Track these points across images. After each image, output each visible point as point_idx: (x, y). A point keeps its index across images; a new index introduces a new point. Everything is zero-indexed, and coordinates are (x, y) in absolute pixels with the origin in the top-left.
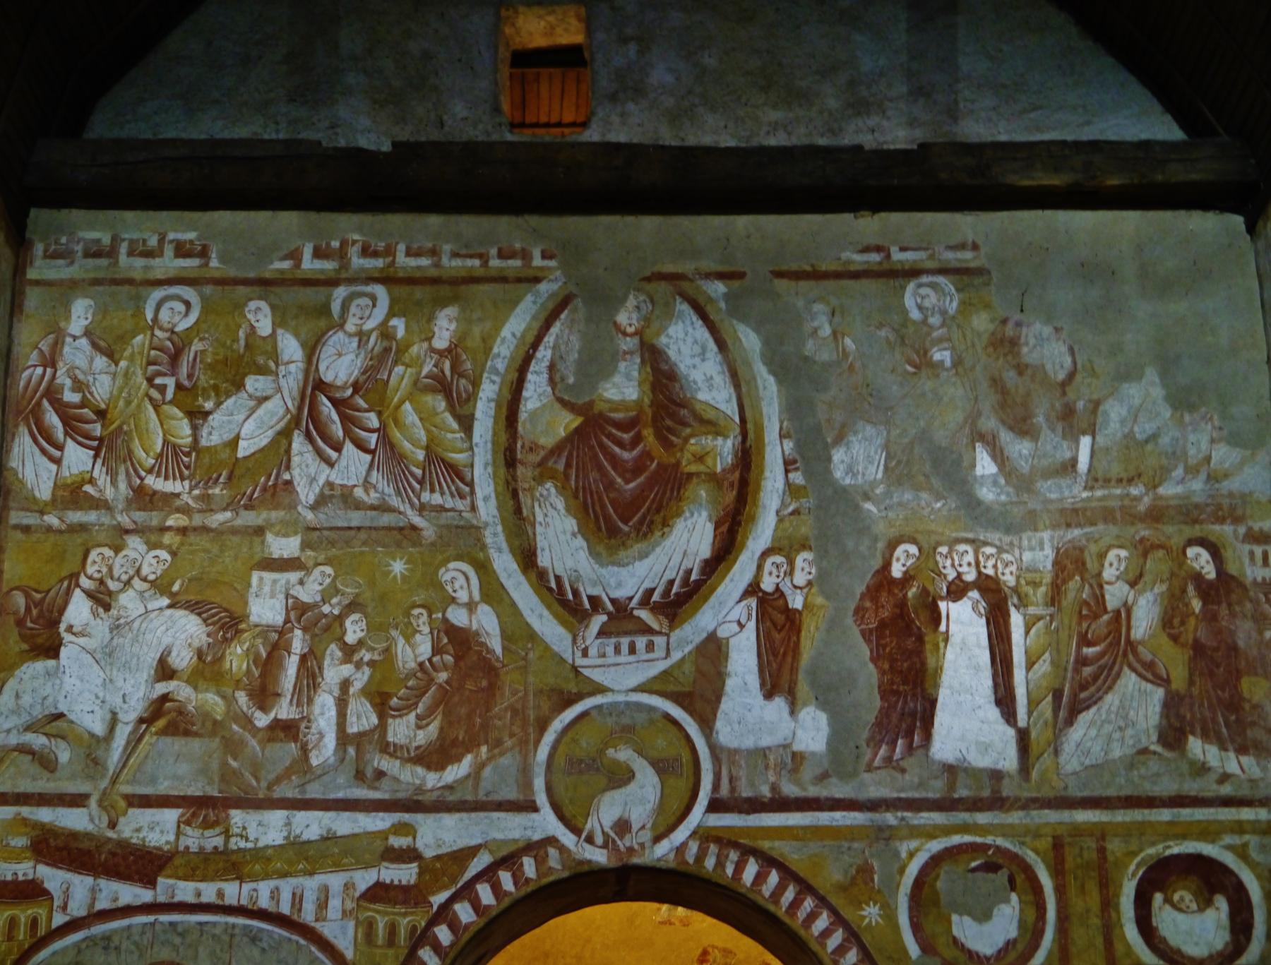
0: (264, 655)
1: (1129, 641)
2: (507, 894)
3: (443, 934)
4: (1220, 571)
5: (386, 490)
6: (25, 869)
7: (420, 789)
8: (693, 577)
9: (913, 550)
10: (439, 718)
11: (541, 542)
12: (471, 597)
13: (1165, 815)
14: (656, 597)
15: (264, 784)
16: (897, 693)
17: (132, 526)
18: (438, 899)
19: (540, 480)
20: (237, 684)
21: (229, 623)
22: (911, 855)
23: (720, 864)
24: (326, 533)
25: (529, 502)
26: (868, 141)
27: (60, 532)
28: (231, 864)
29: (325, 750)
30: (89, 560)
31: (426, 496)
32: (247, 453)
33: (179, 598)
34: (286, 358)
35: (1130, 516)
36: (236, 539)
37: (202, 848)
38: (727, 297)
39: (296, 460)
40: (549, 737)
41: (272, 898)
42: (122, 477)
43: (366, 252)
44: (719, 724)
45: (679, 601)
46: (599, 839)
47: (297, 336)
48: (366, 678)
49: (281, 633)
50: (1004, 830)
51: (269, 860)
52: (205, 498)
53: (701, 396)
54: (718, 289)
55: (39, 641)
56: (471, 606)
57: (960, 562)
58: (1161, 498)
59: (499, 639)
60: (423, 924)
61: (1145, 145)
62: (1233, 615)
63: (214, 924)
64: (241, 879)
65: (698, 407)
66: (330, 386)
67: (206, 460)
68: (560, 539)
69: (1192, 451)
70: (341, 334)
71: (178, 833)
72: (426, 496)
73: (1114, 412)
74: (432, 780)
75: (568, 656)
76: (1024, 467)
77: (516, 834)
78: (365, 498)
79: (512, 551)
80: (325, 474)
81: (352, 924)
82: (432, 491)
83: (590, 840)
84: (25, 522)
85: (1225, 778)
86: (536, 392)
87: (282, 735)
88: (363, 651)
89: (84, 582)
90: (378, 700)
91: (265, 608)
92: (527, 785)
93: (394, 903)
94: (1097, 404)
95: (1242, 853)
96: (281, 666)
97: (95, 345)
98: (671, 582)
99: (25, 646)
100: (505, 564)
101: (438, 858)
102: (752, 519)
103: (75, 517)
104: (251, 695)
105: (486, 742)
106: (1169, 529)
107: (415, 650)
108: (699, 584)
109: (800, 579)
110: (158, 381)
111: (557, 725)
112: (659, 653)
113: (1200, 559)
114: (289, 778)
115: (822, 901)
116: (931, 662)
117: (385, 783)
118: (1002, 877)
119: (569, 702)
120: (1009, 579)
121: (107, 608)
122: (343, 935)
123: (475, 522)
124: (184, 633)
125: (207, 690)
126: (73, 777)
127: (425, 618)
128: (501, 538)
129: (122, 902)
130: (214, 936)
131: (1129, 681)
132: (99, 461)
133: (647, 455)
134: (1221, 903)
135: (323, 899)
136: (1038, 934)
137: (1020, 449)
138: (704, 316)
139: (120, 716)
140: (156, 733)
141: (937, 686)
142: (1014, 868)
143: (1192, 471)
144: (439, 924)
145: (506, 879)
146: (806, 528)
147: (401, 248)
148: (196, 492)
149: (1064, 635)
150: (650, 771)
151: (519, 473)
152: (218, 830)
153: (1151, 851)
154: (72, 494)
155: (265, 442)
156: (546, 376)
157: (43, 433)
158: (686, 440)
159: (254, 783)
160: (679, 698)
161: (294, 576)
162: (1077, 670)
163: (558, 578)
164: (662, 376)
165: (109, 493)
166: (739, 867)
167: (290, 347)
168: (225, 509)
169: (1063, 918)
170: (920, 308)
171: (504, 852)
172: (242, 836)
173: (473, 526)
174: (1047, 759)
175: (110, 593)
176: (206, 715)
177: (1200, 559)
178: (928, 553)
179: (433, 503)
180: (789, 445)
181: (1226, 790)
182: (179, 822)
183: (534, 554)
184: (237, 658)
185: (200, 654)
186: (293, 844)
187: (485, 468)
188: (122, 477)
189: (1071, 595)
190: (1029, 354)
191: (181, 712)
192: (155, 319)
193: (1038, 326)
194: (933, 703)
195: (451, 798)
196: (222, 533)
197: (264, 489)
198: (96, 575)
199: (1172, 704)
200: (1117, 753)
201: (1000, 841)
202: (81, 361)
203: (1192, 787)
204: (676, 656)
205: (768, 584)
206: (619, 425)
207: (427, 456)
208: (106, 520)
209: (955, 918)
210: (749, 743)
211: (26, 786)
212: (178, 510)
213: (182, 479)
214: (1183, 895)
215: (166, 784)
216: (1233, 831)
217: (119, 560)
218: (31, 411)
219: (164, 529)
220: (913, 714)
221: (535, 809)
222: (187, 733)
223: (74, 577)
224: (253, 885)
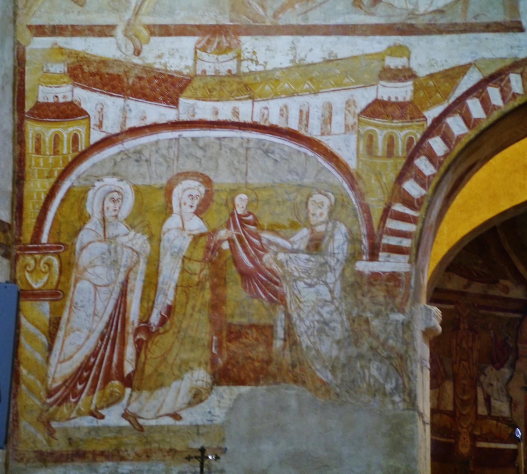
2: (495, 108)
3: (437, 145)
6: (65, 92)
15: (270, 13)
28: (244, 86)
37: (216, 71)
41: (282, 115)
51: (277, 81)
60: (419, 136)
63: (231, 139)
71: (196, 59)
77: (503, 53)
81: (354, 137)
101: (431, 76)
114: (293, 6)
129: (149, 121)
130: (231, 149)
135: (327, 115)
144: (433, 136)
145: (494, 94)
152: (231, 55)
159: (261, 11)
171: (492, 70)
172: (252, 60)
182: (196, 48)
186: (298, 66)
195: (442, 21)
215: (182, 14)
224: (264, 104)
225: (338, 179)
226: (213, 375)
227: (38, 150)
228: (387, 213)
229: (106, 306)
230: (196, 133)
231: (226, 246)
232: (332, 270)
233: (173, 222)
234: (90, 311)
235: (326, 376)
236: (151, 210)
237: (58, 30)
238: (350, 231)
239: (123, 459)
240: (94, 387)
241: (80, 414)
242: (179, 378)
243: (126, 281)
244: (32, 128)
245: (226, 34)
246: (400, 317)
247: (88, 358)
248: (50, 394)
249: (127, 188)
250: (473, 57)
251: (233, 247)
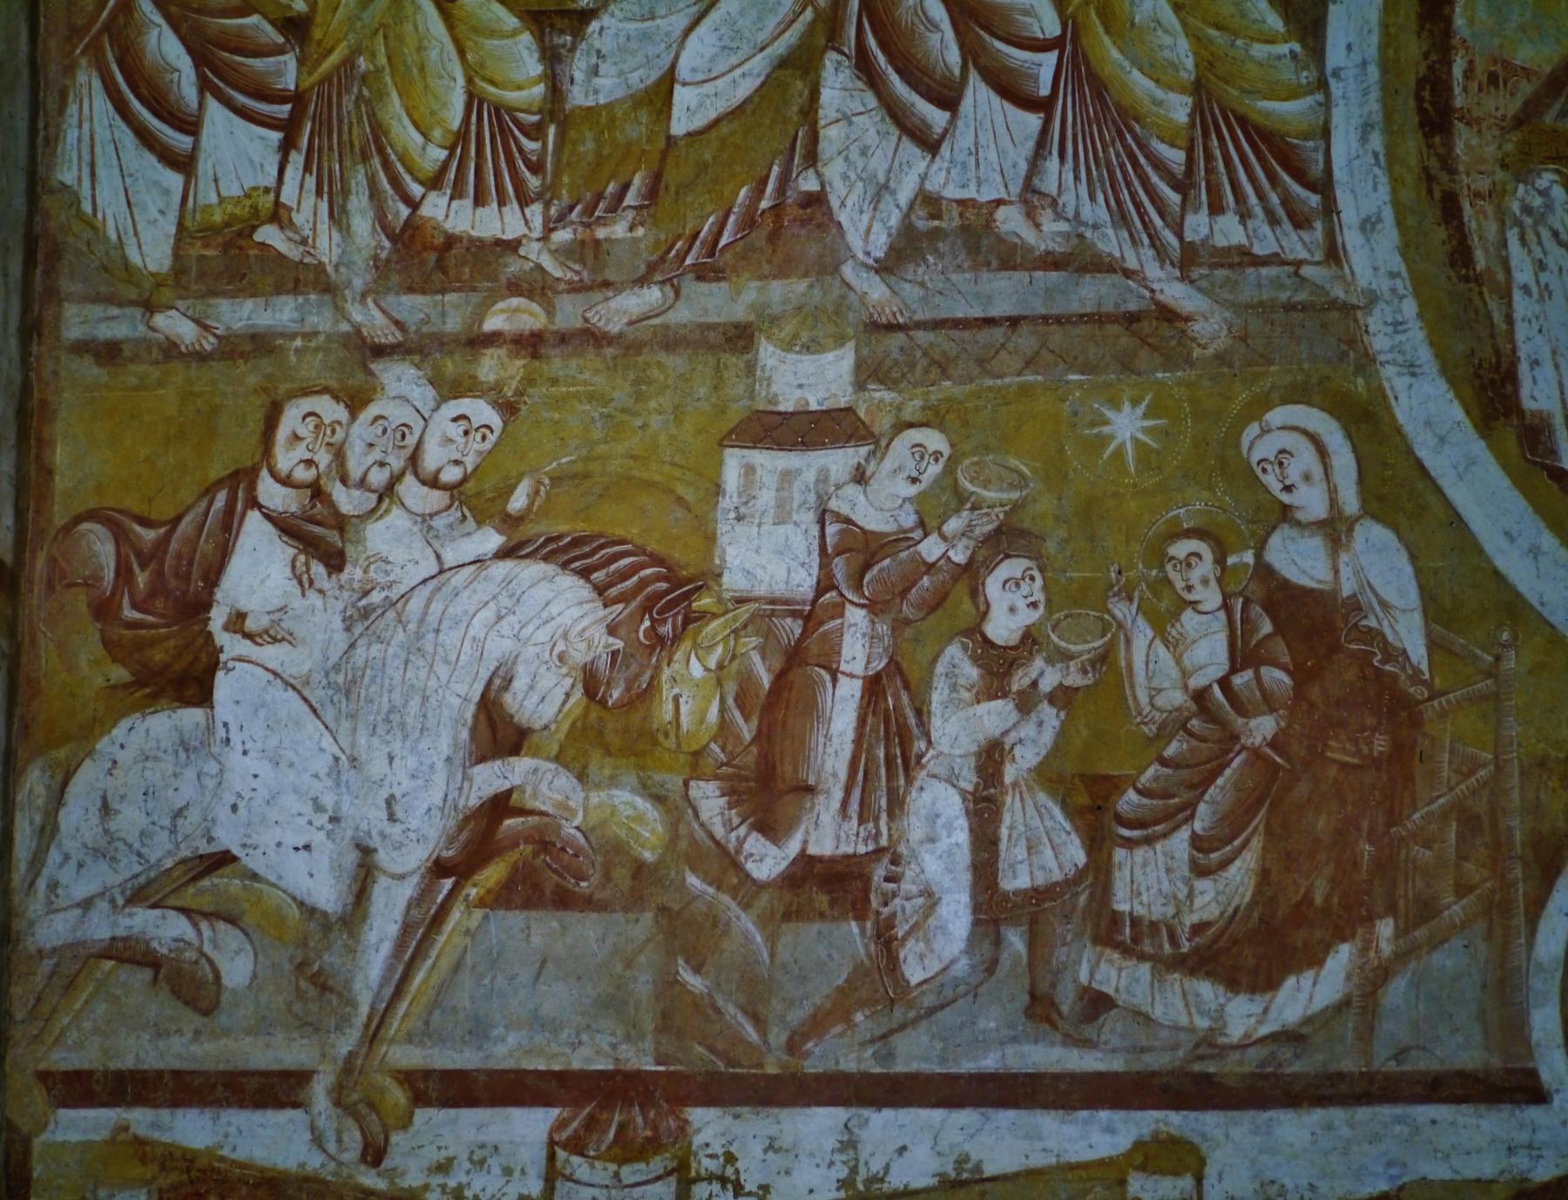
0: (766, 680)
5: (1087, 212)
7: (1209, 1044)
10: (1257, 843)
11: (1528, 341)
12: (1333, 503)
15: (778, 1037)
17: (392, 336)
19: (1521, 166)
20: (696, 764)
21: (667, 597)
24: (922, 337)
25: (1492, 228)
27: (201, 357)
29: (943, 941)
30: (282, 433)
31: (1198, 224)
32: (699, 122)
33: (529, 529)
36: (676, 362)
39: (831, 136)
42: (359, 202)
48: (1048, 737)
49: (811, 619)
52: (588, 251)
55: (158, 656)
56: (1335, 530)
59: (1417, 619)
67: (588, 146)
72: (1198, 224)
74: (1242, 1016)
78: (1029, 235)
79: (1444, 371)
80: (914, 172)
82: (1216, 208)
84: (105, 332)
87: (822, 900)
88: (1039, 663)
89: (270, 492)
90: (1083, 799)
91: (765, 555)
92: (1514, 1029)
96: (811, 710)
99: (120, 674)
100: (1427, 407)
103: (240, 314)
104: (734, 793)
105: (1392, 910)
107: (1183, 655)
114: (846, 1017)
117: (1111, 1027)
121: (335, 561)
123: (1339, 292)
124: (547, 627)
125: (613, 782)
126: (262, 1027)
127: (1206, 567)
128: (1416, 335)
132: (297, 159)
139: (383, 857)
140: (481, 903)
148: (563, 236)
151: (1459, 148)
152: (658, 1164)
154: (227, 252)
155: (746, 88)
157: (142, 88)
161: (839, 461)
165: (327, 246)
168: (642, 281)
172: (723, 1180)
173: (1333, 304)
175: (341, 523)
176: (615, 851)
179: (1220, 241)
182: (552, 1143)
183: (1511, 377)
184: (691, 692)
185: (591, 682)
187: (1364, 139)
188: (359, 202)
191: (544, 842)
196: (636, 347)
197: (749, 222)
198: (302, 474)
207: (1198, 110)
208: (322, 320)
211: (139, 1052)
212: (514, 288)
213: (524, 200)
215: (512, 1040)
217: (362, 429)
218: (107, 28)
219: (479, 342)
222: (564, 900)
223: (242, 481)
245: (646, 1102)
250: (1392, 1178)
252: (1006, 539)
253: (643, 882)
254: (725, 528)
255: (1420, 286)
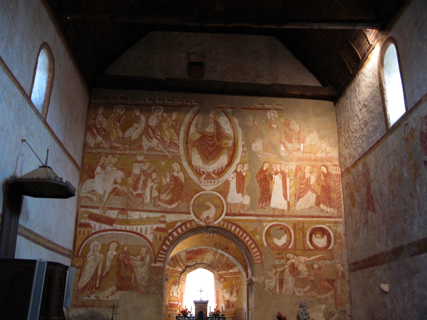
1: (310, 185)
3: (171, 238)
4: (328, 172)
6: (86, 221)
7: (167, 209)
8: (224, 168)
9: (268, 165)
11: (193, 160)
13: (316, 219)
14: (216, 172)
16: (264, 193)
18: (170, 231)
19: (193, 147)
21: (129, 173)
22: (266, 226)
23: (227, 226)
26: (261, 83)
27: (96, 153)
28: (128, 222)
31: (169, 149)
34: (142, 120)
35: (311, 160)
37: (122, 219)
38: (232, 112)
39: (143, 141)
40: (193, 199)
42: (108, 143)
43: (159, 100)
44: (228, 198)
45: (221, 173)
46: (203, 220)
47: (145, 116)
50: (284, 221)
51: (136, 221)
53: (226, 132)
54: (230, 110)
56: (178, 172)
57: (277, 168)
58: (316, 157)
61: (315, 87)
62: (330, 180)
64: (130, 225)
65: (225, 134)
66: (151, 126)
68: (197, 160)
69: (323, 148)
70: (153, 116)
71: (118, 215)
73: (308, 139)
74: (169, 207)
75: (198, 183)
76: (290, 149)
77: (186, 219)
80: (149, 144)
81: (152, 236)
83: (201, 220)
84: (88, 151)
85: (327, 212)
86: (193, 129)
89: (100, 164)
93: (161, 231)
94: (305, 137)
95: (330, 227)
96: (139, 183)
97: (104, 116)
98: (219, 169)
99: (88, 176)
100: (185, 164)
101: (170, 223)
102: (236, 157)
103: (99, 150)
104: (133, 188)
106: (318, 163)
107: (167, 180)
108: (225, 170)
109: (245, 169)
110: (116, 124)
111: (195, 197)
112: (216, 183)
113: (324, 169)
115: (248, 234)
116: (271, 187)
118: (284, 231)
119: (197, 192)
120: (287, 171)
121: (104, 169)
122: (150, 237)
124: (120, 175)
128: (185, 159)
131: (309, 193)
133: (215, 143)
134: (326, 237)
136: (290, 242)
137: (289, 145)
138: (227, 116)
139: (107, 191)
141: (272, 192)
142: (286, 229)
143: (322, 152)
145: (184, 227)
146: (246, 159)
147: (166, 99)
149: (297, 183)
150: (214, 207)
153: (313, 226)
154: (98, 146)
156: (195, 126)
158: (223, 140)
160: (220, 193)
161: (142, 164)
162: (299, 190)
163: (196, 167)
164: (218, 127)
165: (105, 146)
166: (231, 227)
167: (143, 118)
169: (295, 239)
170: (270, 116)
171: (184, 222)
174: (293, 208)
175: (105, 166)
177: (324, 169)
178: (271, 165)
180: (243, 142)
181: (327, 215)
184: (130, 181)
185: (123, 179)
188: (108, 143)
189: (299, 175)
190: (292, 127)
191: (119, 191)
192: (116, 111)
193: (293, 121)
194: (271, 196)
195: (173, 211)
197: (137, 147)
199: (317, 198)
200: (307, 207)
201: (283, 224)
202: (101, 119)
203: (321, 214)
204: (220, 184)
205: (238, 170)
206: (209, 137)
209: (274, 238)
210: (234, 202)
212: (119, 150)
214: (318, 235)
216: (328, 223)
217: (107, 160)
220: (267, 198)
221: (190, 213)
222: (120, 195)
223: (98, 162)
225: (148, 244)
226: (117, 288)
227: (80, 234)
228: (159, 253)
229: (93, 271)
230: (117, 232)
231: (122, 258)
232: (146, 265)
233: (110, 252)
234: (89, 272)
235: (142, 289)
236: (105, 250)
237: (86, 207)
238: (150, 257)
239: (94, 307)
240: (89, 290)
241: (85, 296)
242: (109, 288)
243: (98, 265)
244: (79, 229)
246: (160, 277)
247: (88, 283)
248: (78, 291)
249: (99, 244)
251: (123, 259)
252: (154, 171)
253: (126, 194)
254: (133, 169)
255: (185, 155)
